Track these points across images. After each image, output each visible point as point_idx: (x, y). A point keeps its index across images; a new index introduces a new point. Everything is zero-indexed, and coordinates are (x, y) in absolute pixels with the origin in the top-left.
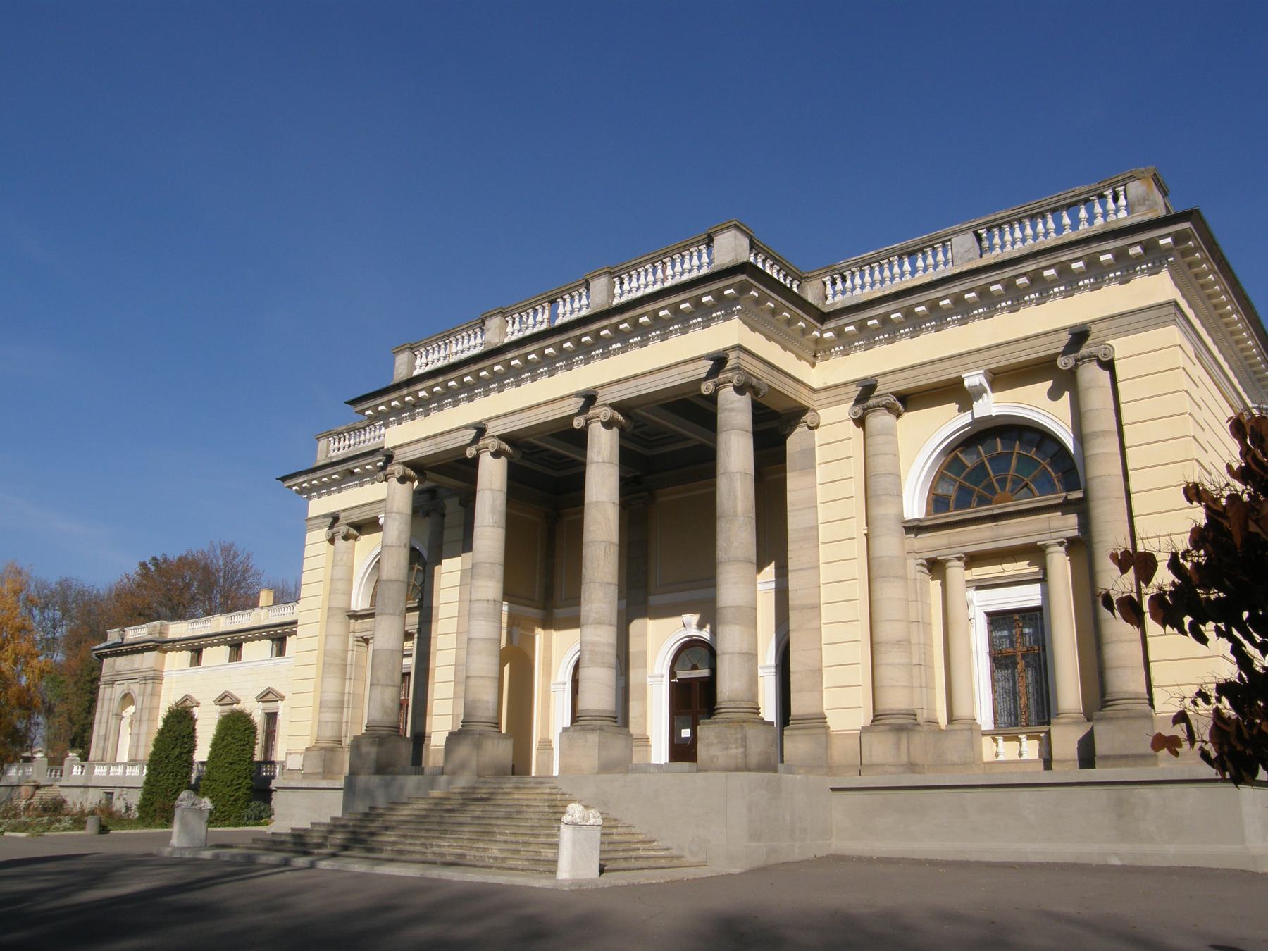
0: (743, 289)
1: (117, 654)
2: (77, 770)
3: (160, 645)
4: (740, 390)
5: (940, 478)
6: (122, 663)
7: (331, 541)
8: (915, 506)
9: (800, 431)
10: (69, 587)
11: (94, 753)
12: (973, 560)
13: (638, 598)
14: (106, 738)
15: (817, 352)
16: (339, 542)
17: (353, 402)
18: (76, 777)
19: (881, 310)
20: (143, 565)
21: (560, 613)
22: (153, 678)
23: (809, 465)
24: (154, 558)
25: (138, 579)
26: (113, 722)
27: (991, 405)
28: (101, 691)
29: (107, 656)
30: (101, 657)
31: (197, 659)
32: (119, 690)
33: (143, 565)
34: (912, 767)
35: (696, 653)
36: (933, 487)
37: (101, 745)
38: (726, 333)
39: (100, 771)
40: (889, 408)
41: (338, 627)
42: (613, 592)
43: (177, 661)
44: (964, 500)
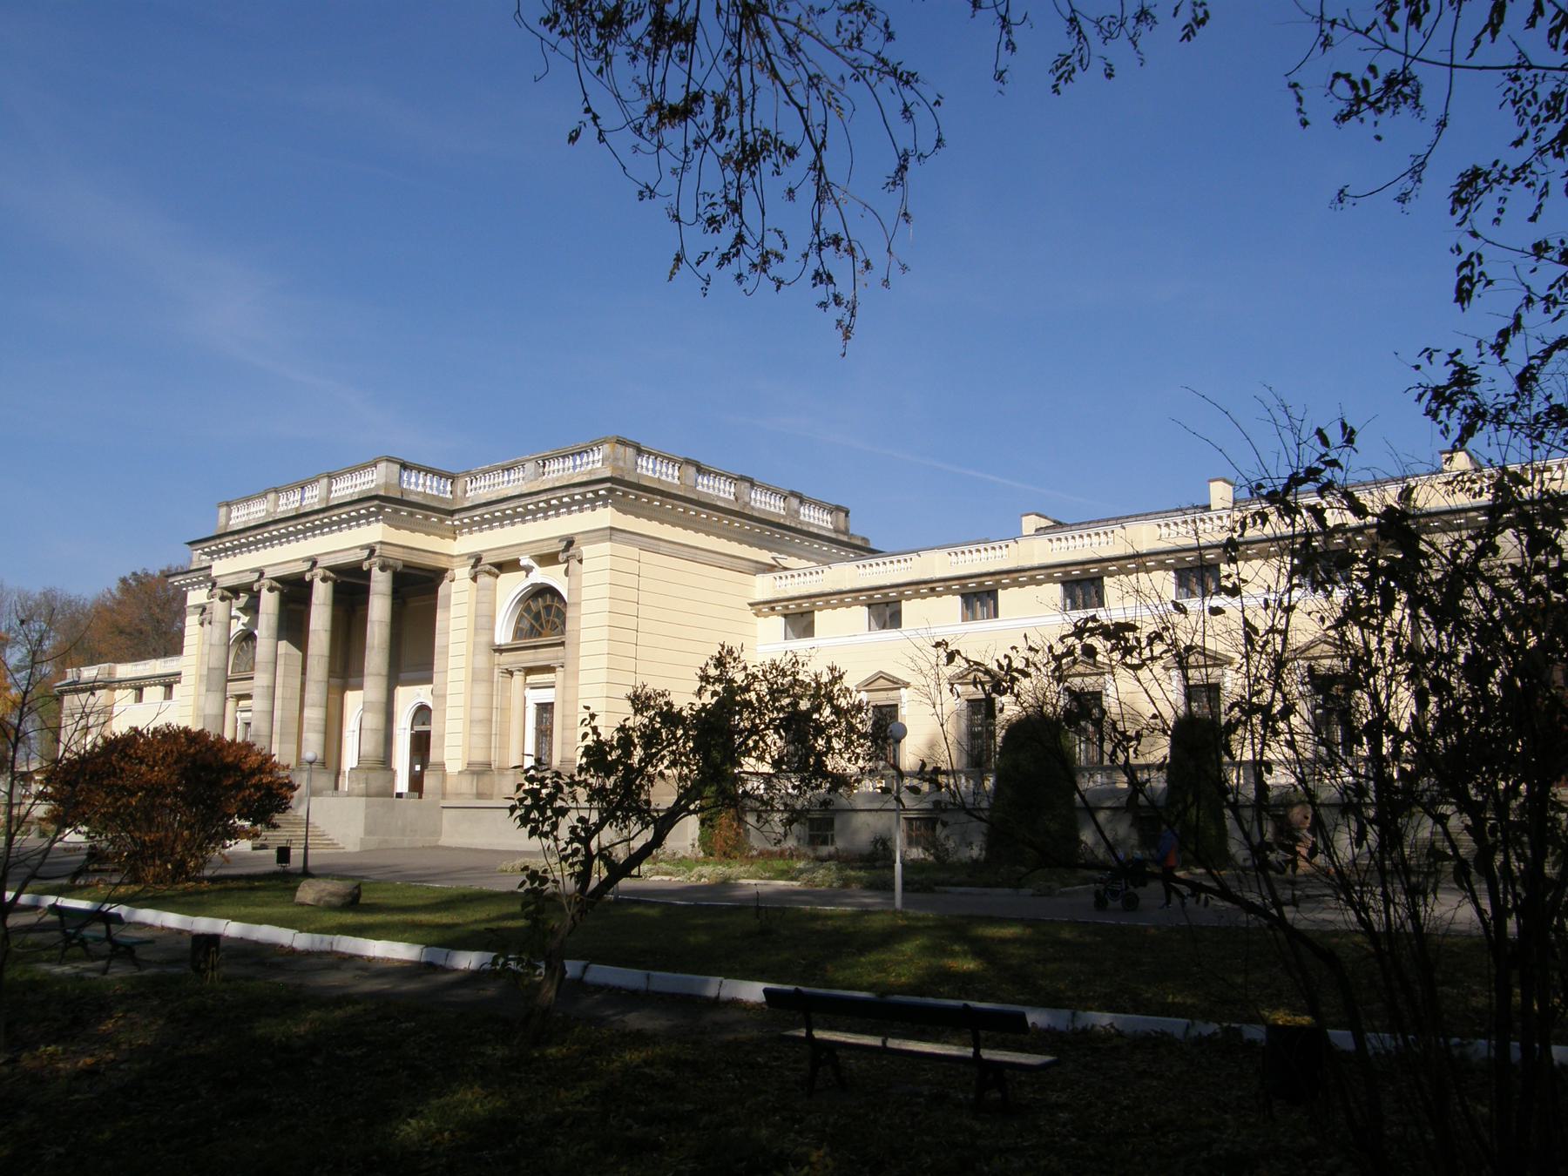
0: (380, 508)
1: (77, 691)
3: (110, 684)
4: (383, 568)
5: (521, 618)
7: (202, 624)
8: (503, 635)
9: (446, 581)
10: (54, 598)
12: (529, 671)
13: (395, 677)
15: (454, 533)
16: (206, 626)
17: (190, 544)
19: (479, 512)
20: (124, 581)
21: (352, 681)
23: (448, 607)
24: (134, 574)
25: (118, 595)
27: (541, 575)
29: (70, 691)
30: (62, 693)
31: (139, 698)
33: (124, 581)
34: (479, 796)
35: (423, 713)
36: (518, 622)
38: (375, 532)
40: (489, 573)
42: (323, 686)
43: (124, 697)
44: (534, 632)
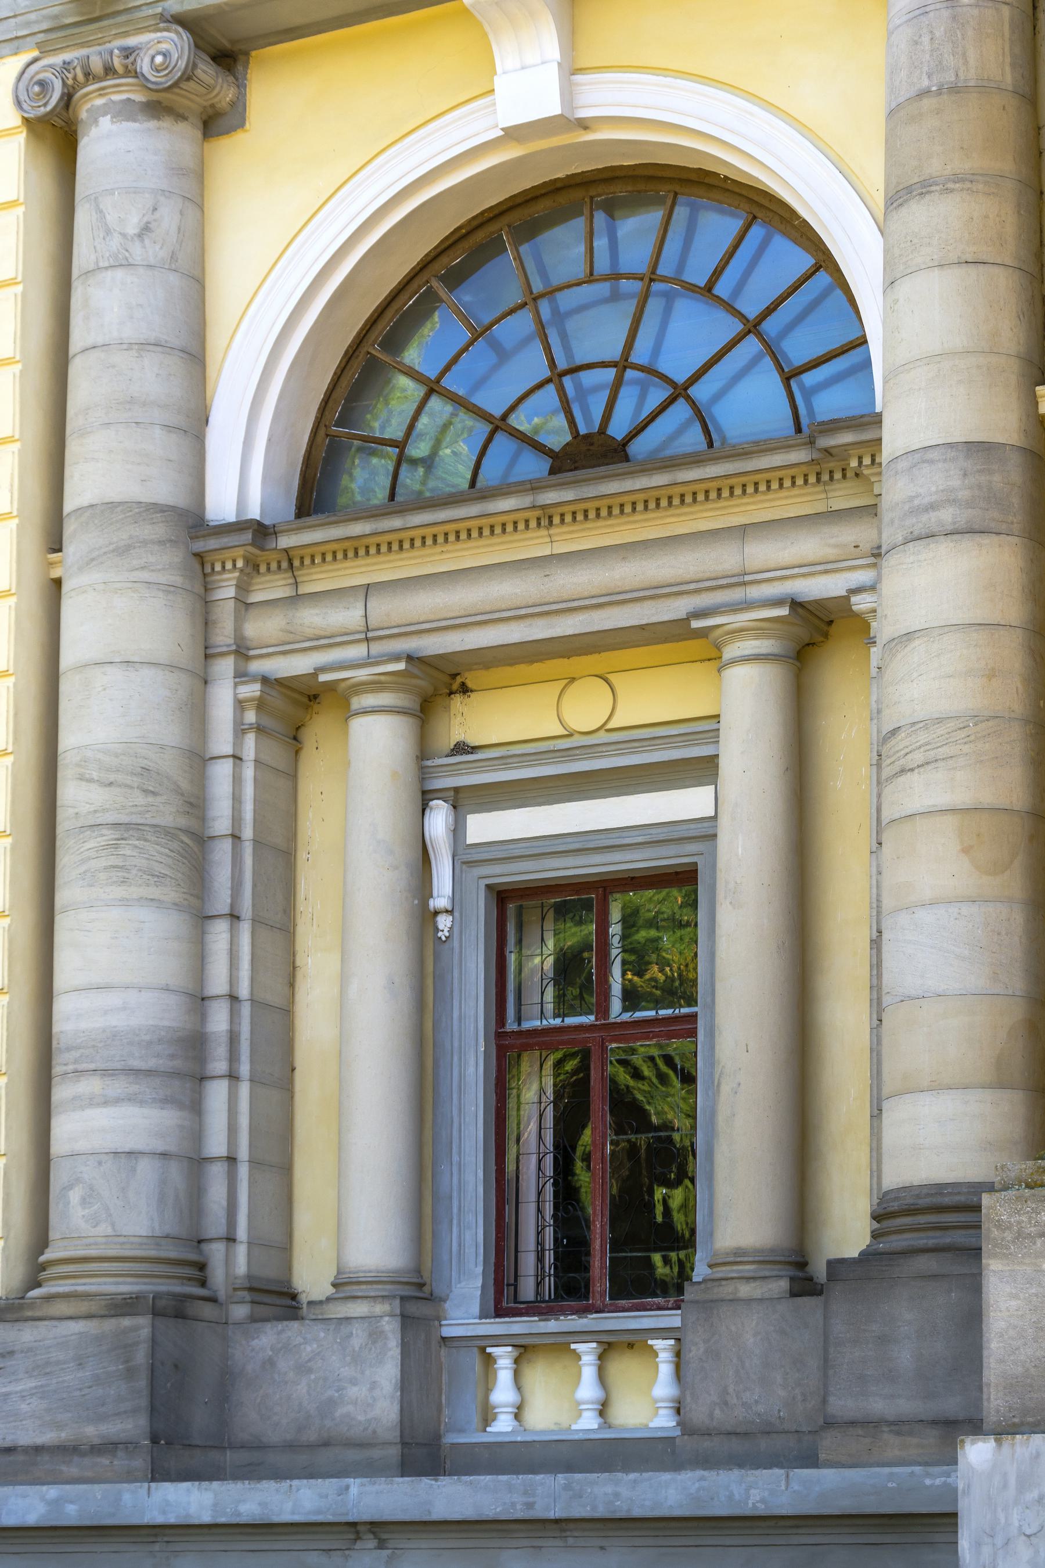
41: (119, 617)
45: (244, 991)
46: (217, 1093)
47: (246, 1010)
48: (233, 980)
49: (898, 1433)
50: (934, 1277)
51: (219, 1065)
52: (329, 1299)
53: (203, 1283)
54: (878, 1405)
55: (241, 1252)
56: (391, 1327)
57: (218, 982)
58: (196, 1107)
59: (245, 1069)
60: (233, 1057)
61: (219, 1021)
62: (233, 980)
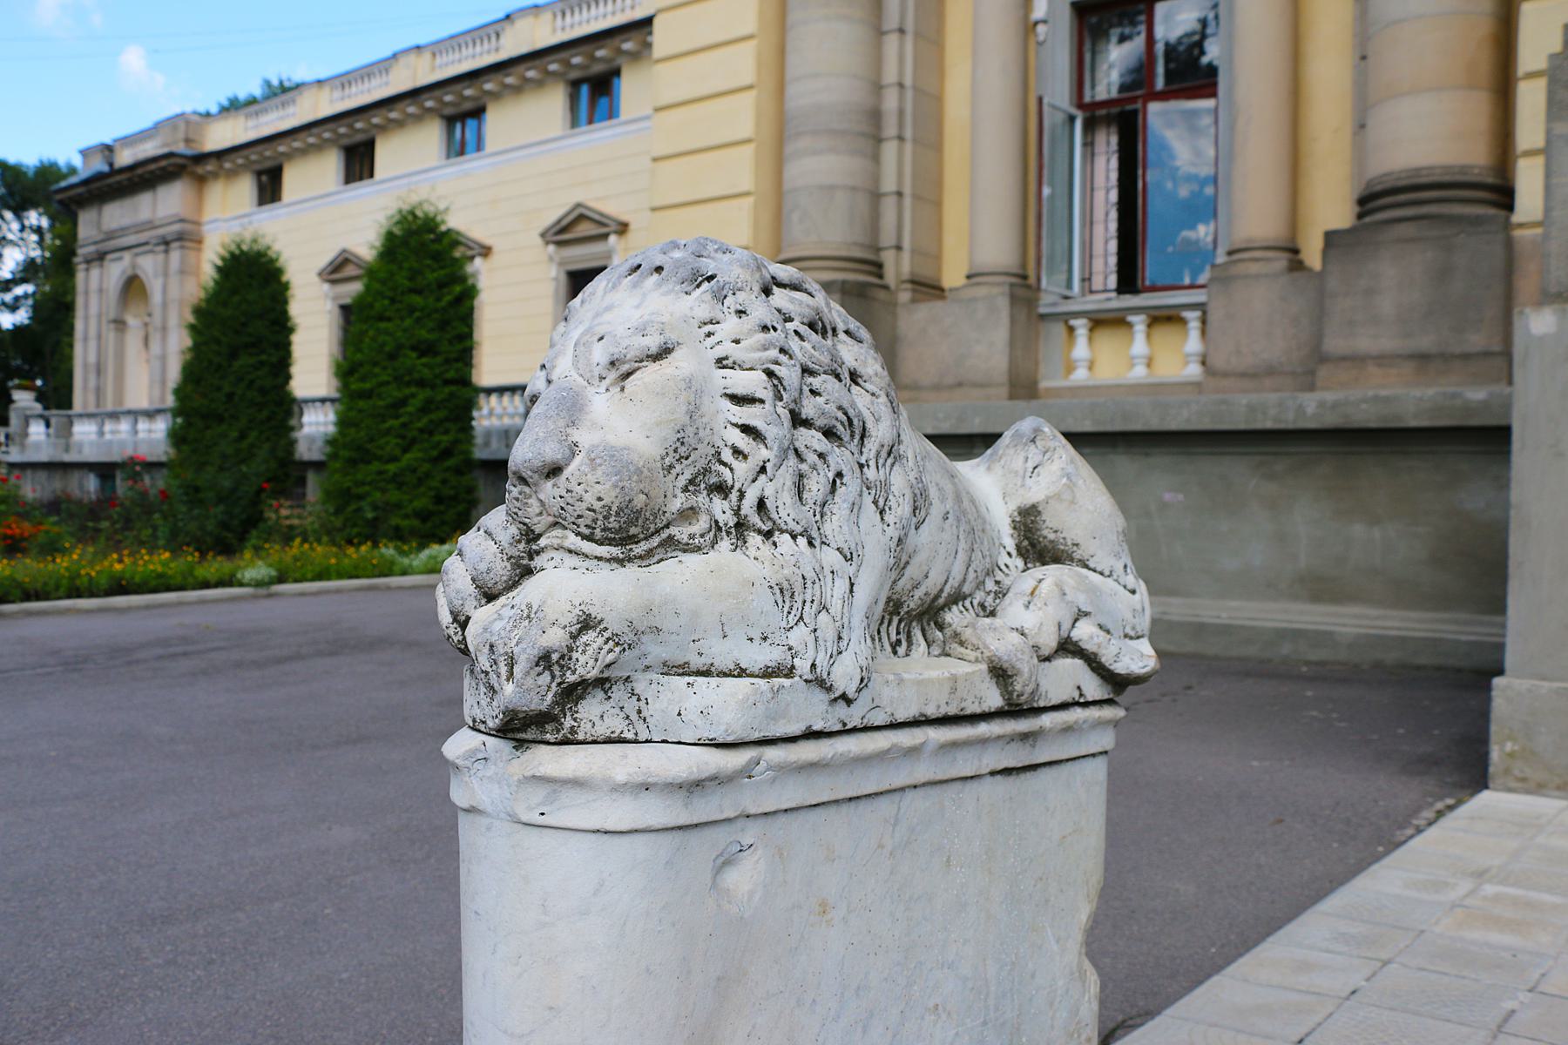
2: (37, 430)
6: (116, 215)
11: (81, 398)
14: (99, 370)
18: (37, 445)
22: (180, 237)
26: (111, 336)
28: (80, 276)
32: (115, 271)
37: (92, 383)
39: (84, 431)
45: (908, 81)
46: (889, 150)
47: (909, 94)
48: (901, 73)
49: (1379, 365)
50: (1412, 240)
51: (890, 129)
52: (965, 286)
53: (881, 276)
54: (1364, 343)
55: (906, 256)
56: (1003, 304)
57: (890, 75)
58: (876, 158)
59: (908, 133)
60: (901, 125)
61: (890, 102)
62: (901, 73)
